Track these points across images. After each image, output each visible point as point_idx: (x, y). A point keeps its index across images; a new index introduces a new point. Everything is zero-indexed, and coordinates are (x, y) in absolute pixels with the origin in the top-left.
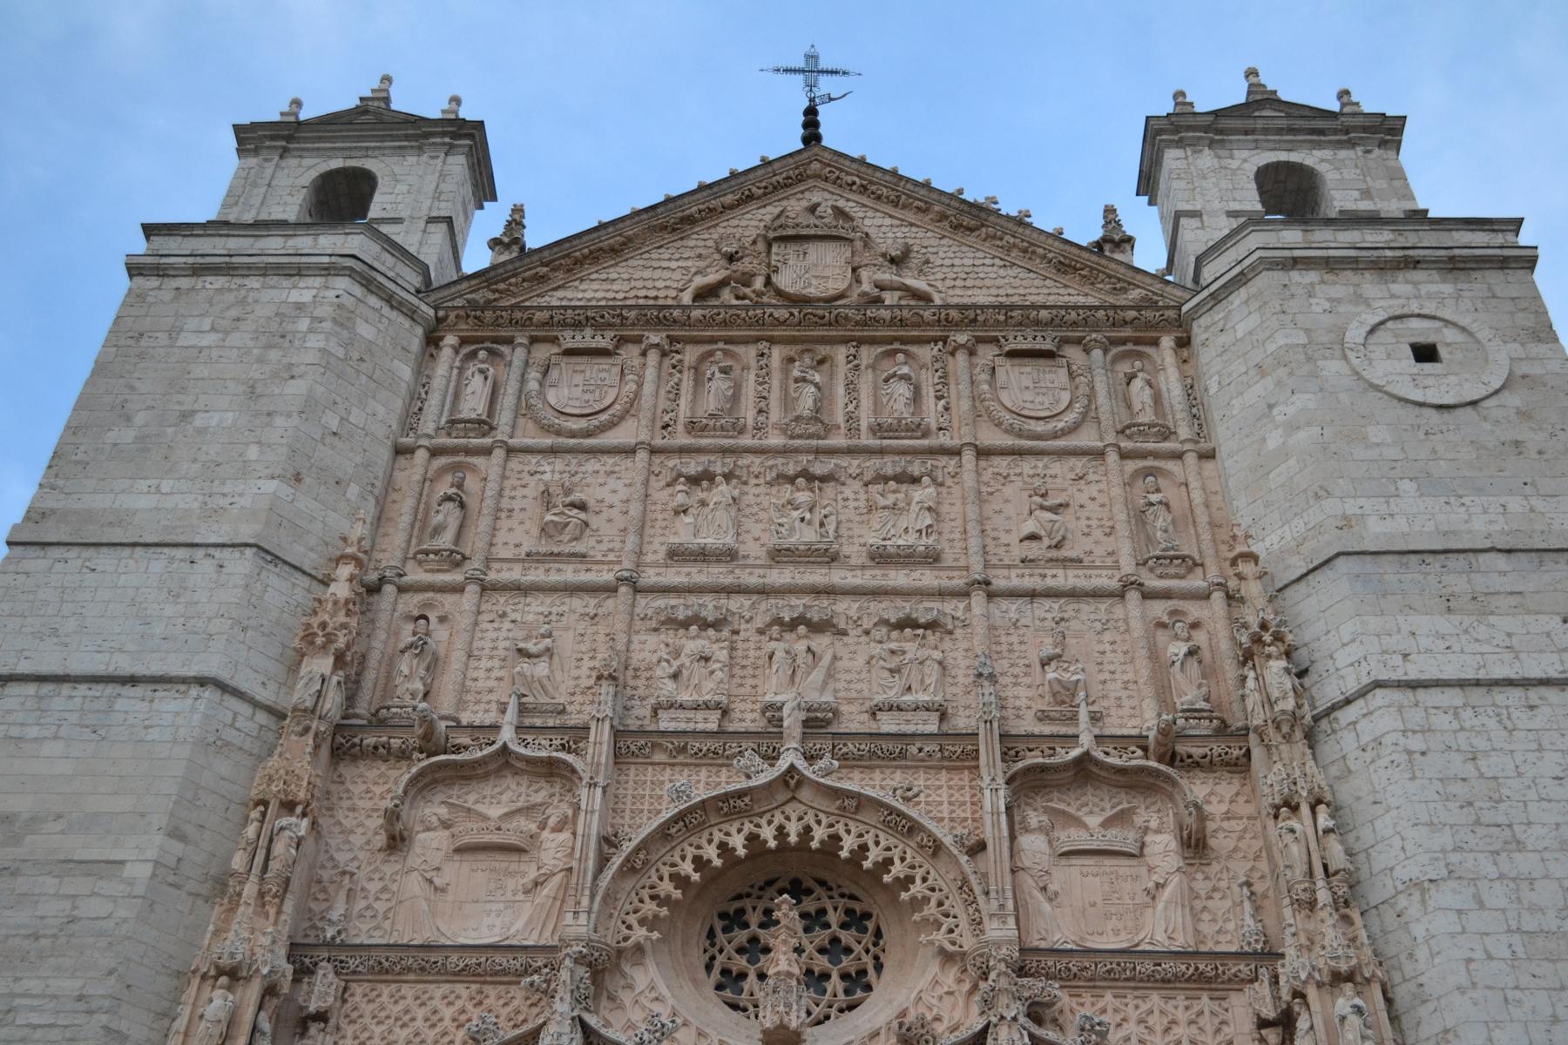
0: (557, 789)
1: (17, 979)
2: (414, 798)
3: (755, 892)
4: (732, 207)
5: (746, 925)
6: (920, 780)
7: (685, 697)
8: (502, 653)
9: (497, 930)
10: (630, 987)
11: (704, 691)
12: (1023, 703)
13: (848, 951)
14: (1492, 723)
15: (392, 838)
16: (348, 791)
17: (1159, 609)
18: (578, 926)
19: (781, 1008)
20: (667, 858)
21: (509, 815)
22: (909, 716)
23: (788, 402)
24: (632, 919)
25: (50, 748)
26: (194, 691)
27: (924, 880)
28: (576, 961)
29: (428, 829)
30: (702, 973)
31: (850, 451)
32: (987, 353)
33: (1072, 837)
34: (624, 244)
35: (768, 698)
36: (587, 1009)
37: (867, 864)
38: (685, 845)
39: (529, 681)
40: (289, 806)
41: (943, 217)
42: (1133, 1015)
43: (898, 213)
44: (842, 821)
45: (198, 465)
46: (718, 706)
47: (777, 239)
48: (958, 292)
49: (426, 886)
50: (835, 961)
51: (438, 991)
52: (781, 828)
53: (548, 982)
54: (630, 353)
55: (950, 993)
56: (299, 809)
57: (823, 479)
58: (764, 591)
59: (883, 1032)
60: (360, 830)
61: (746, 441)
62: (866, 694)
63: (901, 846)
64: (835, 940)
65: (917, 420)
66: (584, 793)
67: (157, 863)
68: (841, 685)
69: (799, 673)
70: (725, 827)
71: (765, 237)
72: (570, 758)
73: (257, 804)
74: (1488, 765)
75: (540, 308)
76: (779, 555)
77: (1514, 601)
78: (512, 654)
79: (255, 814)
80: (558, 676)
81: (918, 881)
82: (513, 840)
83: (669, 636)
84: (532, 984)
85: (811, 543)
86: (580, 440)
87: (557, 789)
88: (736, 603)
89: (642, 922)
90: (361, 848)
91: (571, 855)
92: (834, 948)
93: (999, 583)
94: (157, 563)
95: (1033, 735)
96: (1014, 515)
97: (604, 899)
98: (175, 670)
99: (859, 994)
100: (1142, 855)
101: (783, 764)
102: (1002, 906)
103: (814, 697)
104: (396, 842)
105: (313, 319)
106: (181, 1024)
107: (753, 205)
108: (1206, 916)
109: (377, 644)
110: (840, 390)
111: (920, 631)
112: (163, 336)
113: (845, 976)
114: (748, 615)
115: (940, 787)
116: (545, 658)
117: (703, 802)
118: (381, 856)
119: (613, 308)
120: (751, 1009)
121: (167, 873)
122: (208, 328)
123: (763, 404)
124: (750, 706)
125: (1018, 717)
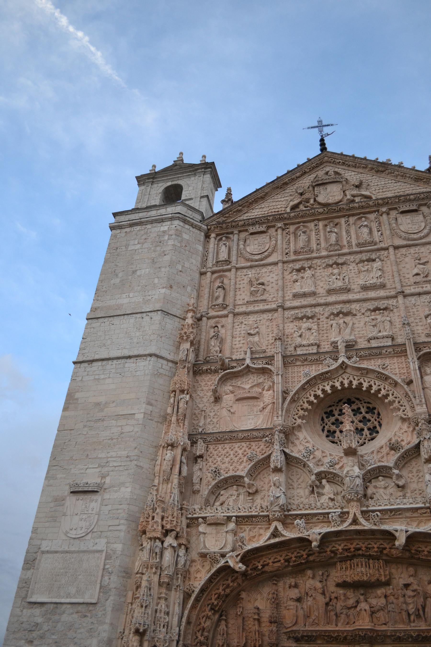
0: (266, 377)
1: (108, 453)
2: (221, 384)
3: (336, 404)
4: (299, 177)
5: (334, 415)
6: (387, 361)
7: (304, 342)
8: (243, 335)
9: (252, 424)
10: (298, 439)
11: (311, 340)
12: (420, 331)
13: (369, 421)
15: (216, 398)
16: (200, 385)
18: (279, 421)
19: (349, 442)
20: (305, 396)
21: (252, 387)
22: (381, 340)
23: (327, 240)
24: (296, 417)
25: (108, 381)
26: (149, 358)
27: (393, 395)
28: (279, 432)
29: (227, 394)
30: (321, 432)
31: (350, 253)
32: (393, 213)
34: (265, 195)
35: (333, 340)
36: (285, 447)
37: (372, 392)
38: (310, 391)
39: (253, 343)
40: (182, 391)
41: (372, 169)
43: (357, 170)
44: (362, 378)
45: (140, 287)
46: (316, 344)
47: (316, 185)
48: (381, 194)
49: (229, 412)
50: (365, 425)
51: (237, 445)
52: (342, 383)
53: (271, 439)
54: (272, 231)
55: (406, 432)
56: (186, 392)
57: (342, 264)
58: (327, 304)
59: (384, 446)
60: (205, 397)
61: (314, 255)
62: (365, 334)
63: (383, 384)
64: (364, 418)
65: (372, 240)
66: (275, 377)
67: (145, 413)
68: (356, 333)
69: (342, 331)
70: (323, 384)
72: (269, 367)
73: (173, 392)
75: (241, 221)
76: (330, 292)
78: (246, 335)
79: (172, 395)
80: (262, 340)
81: (391, 395)
82: (254, 395)
83: (297, 323)
84: (266, 441)
86: (260, 262)
87: (266, 377)
88: (317, 310)
89: (299, 417)
90: (207, 402)
91: (273, 398)
92: (364, 420)
93: (407, 292)
94: (132, 320)
95: (425, 342)
96: (410, 268)
97: (286, 411)
98: (142, 352)
99: (375, 435)
101: (340, 361)
102: (421, 401)
103: (347, 338)
104: (217, 399)
105: (169, 235)
106: (158, 462)
107: (307, 175)
109: (203, 337)
110: (344, 233)
111: (382, 311)
112: (124, 248)
113: (369, 429)
114: (322, 313)
115: (395, 363)
116: (257, 335)
117: (315, 376)
118: (213, 404)
119: (265, 217)
120: (339, 442)
121: (148, 416)
122: (137, 243)
123: (318, 242)
124: (327, 343)
125: (419, 336)
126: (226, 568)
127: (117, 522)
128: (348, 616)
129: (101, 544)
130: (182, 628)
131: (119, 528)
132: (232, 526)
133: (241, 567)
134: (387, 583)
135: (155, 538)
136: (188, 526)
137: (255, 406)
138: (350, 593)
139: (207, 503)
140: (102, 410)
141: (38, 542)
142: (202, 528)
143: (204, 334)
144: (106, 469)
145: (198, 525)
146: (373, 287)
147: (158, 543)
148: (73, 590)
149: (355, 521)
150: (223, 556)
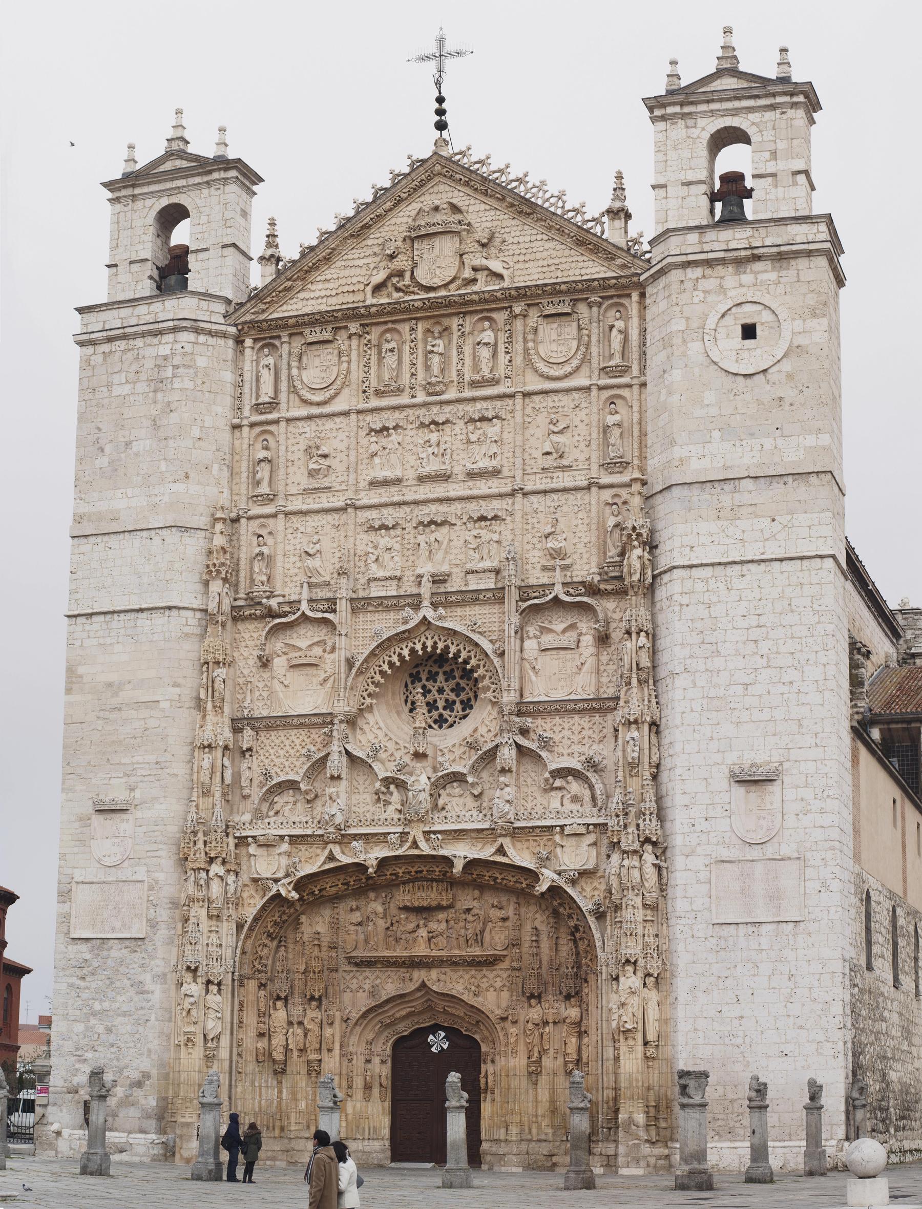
4: (390, 210)
14: (722, 586)
17: (607, 495)
23: (428, 368)
24: (365, 694)
26: (167, 612)
32: (534, 313)
33: (548, 640)
41: (512, 205)
42: (566, 726)
54: (342, 336)
57: (443, 423)
61: (405, 400)
65: (491, 376)
71: (410, 237)
74: (715, 611)
76: (422, 479)
77: (751, 509)
79: (204, 669)
83: (372, 536)
85: (437, 471)
93: (529, 488)
94: (135, 541)
96: (539, 442)
100: (578, 647)
104: (265, 663)
107: (403, 206)
108: (605, 674)
109: (243, 556)
110: (454, 352)
112: (105, 389)
114: (408, 518)
122: (124, 381)
123: (413, 370)
126: (278, 895)
127: (155, 847)
128: (407, 941)
129: (141, 874)
130: (237, 959)
131: (157, 854)
132: (285, 847)
133: (295, 895)
134: (450, 906)
135: (199, 869)
136: (236, 846)
137: (315, 676)
138: (412, 917)
139: (258, 815)
140: (116, 694)
141: (69, 871)
142: (252, 849)
143: (244, 549)
144: (133, 779)
145: (248, 845)
146: (484, 474)
147: (203, 875)
148: (118, 925)
149: (415, 845)
150: (276, 881)
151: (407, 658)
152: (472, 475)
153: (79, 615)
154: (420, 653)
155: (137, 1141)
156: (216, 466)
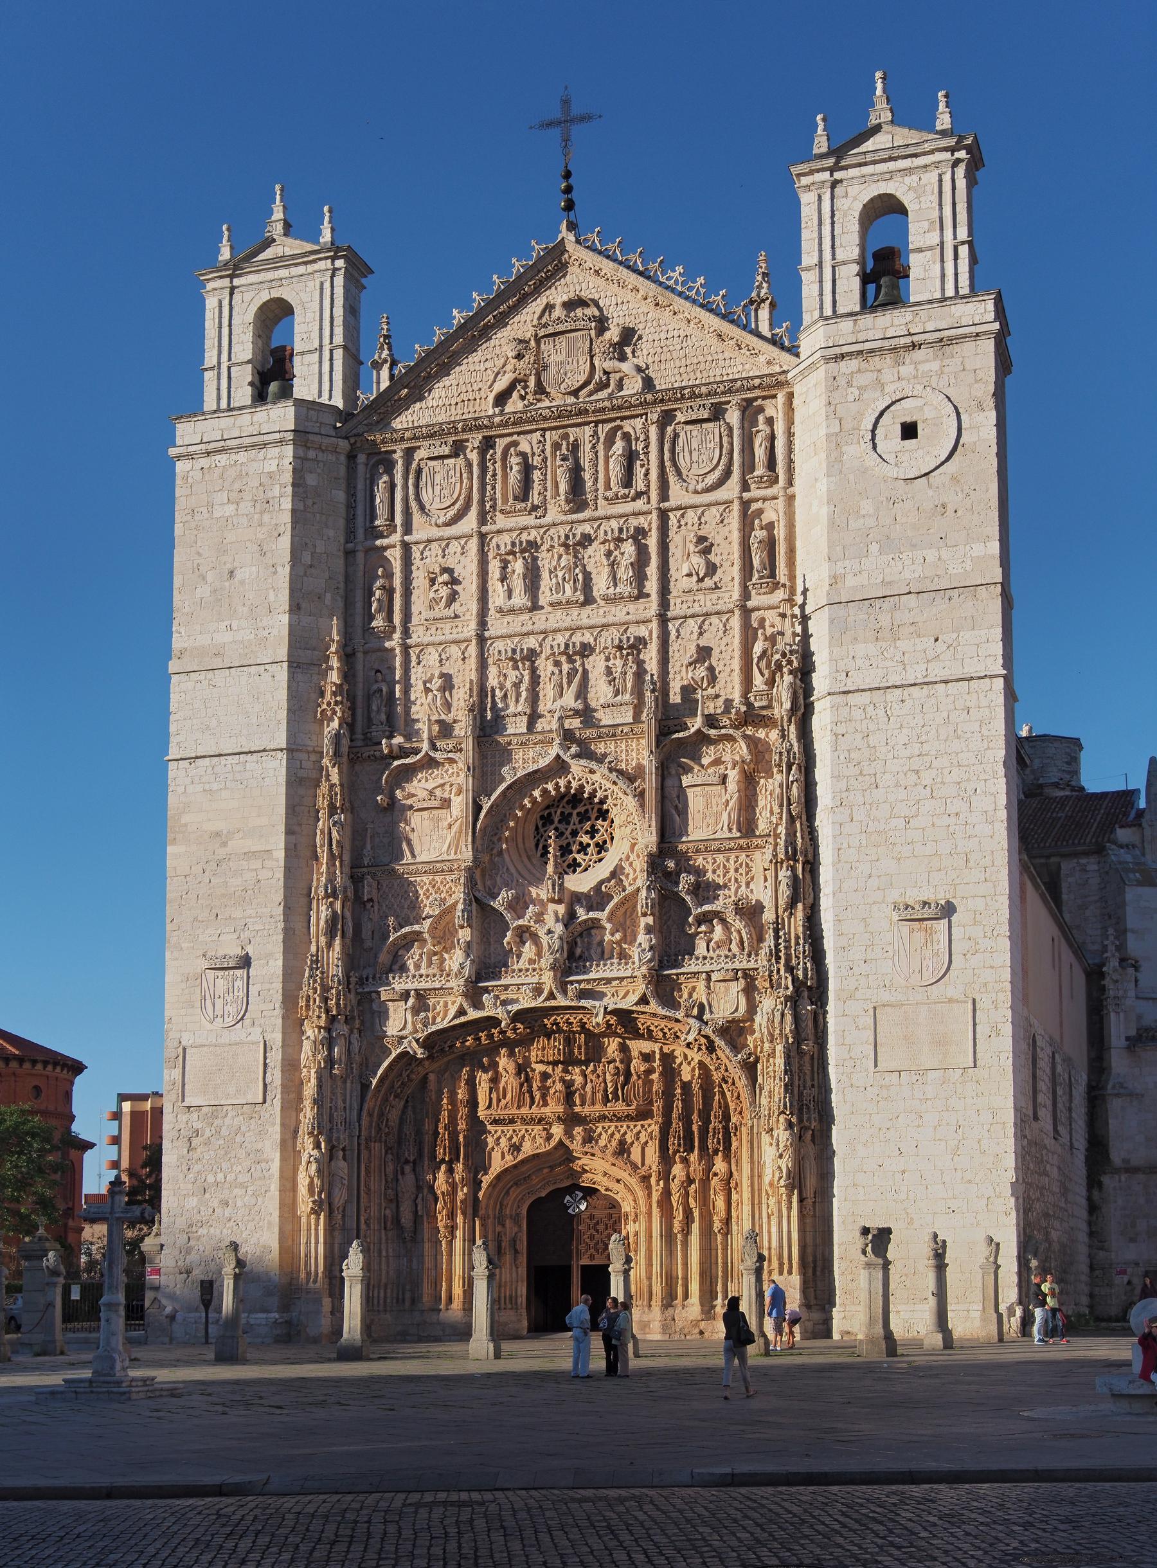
112: (204, 510)
132: (411, 1001)
140: (225, 844)
151: (539, 799)
152: (609, 600)
153: (181, 759)
154: (553, 793)
155: (258, 1322)
156: (328, 596)
